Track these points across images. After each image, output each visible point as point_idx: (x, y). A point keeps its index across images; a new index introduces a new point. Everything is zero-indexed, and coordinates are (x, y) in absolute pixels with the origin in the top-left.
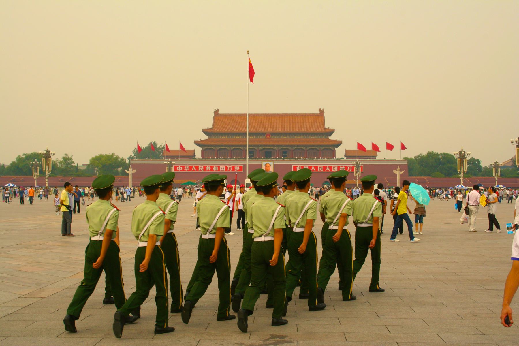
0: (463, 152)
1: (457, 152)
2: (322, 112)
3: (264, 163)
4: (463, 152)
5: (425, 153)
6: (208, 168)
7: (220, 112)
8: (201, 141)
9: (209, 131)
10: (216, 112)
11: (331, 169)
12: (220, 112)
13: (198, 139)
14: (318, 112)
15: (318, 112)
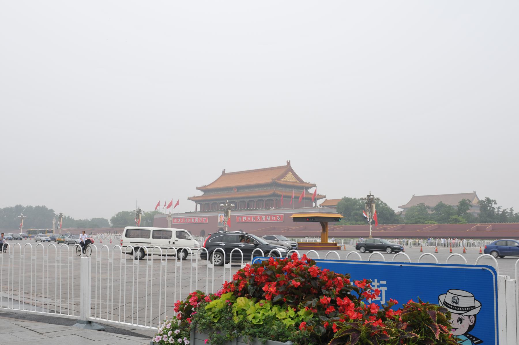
0: (371, 197)
1: (366, 197)
2: (289, 163)
3: (219, 215)
4: (371, 197)
5: (13, 205)
6: (189, 220)
7: (226, 172)
8: (195, 197)
9: (207, 188)
10: (224, 171)
11: (261, 218)
12: (226, 172)
13: (192, 196)
14: (286, 164)
15: (286, 164)
